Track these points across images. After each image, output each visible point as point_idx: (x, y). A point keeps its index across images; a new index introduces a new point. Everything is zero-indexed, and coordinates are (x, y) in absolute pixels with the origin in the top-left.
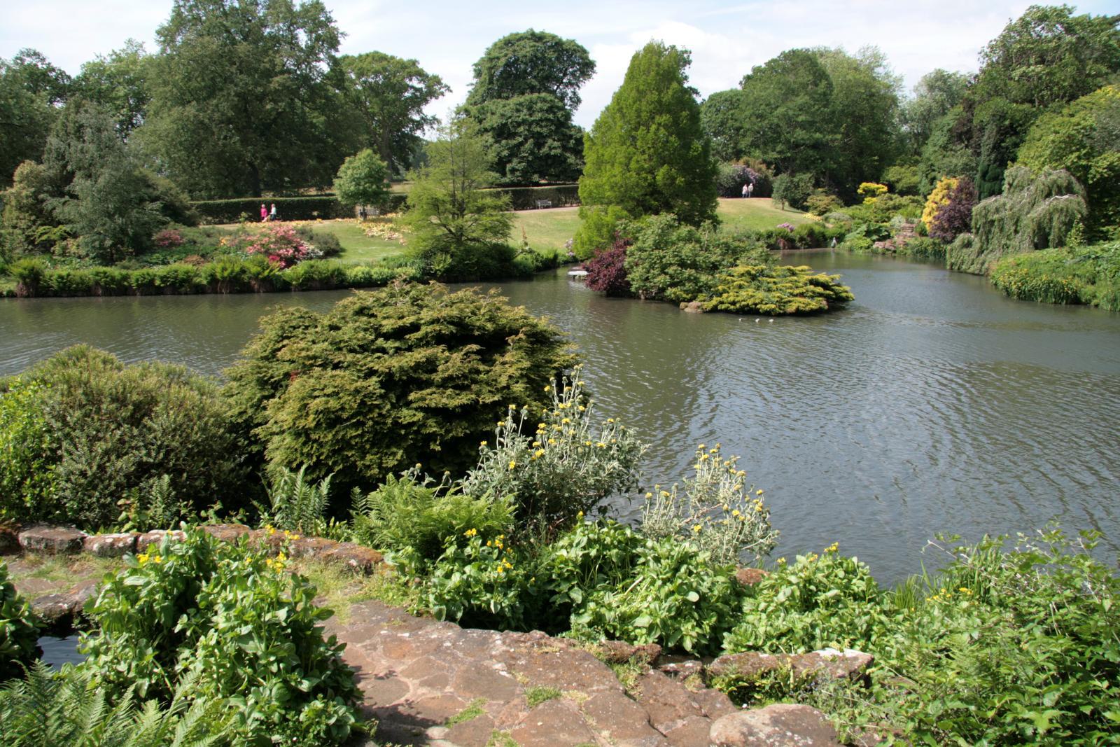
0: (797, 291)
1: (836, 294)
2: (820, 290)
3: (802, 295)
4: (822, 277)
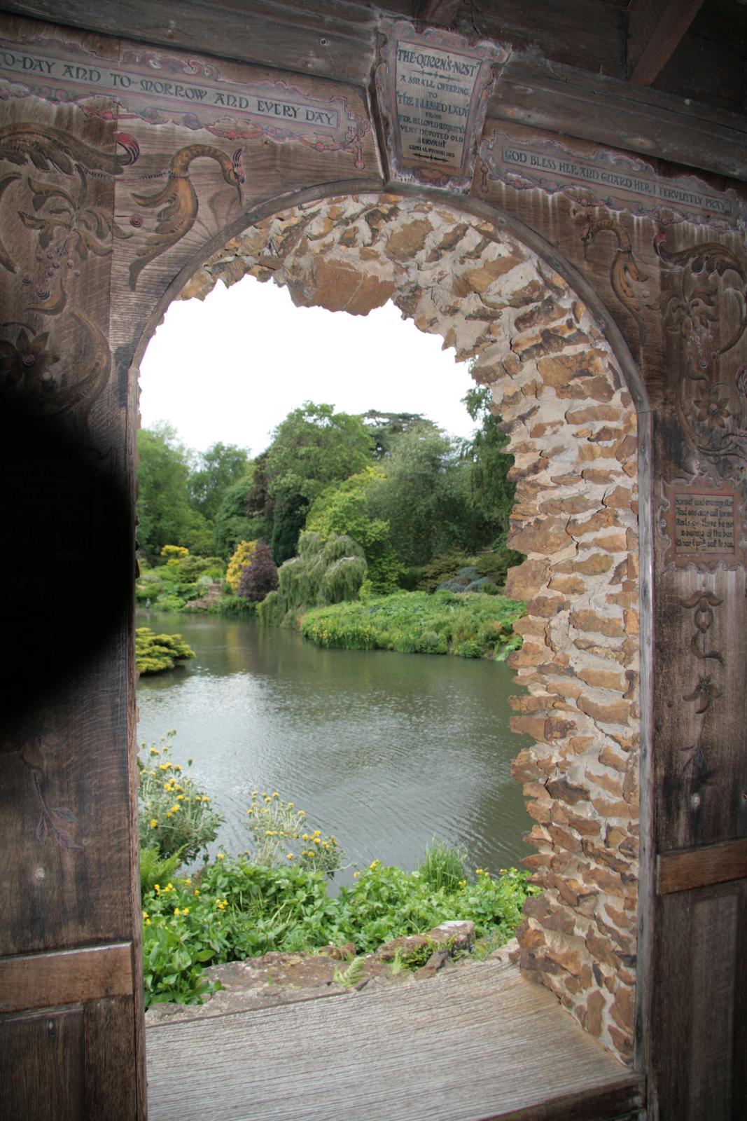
0: (144, 652)
1: (179, 652)
2: (165, 650)
3: (149, 655)
4: (165, 638)
